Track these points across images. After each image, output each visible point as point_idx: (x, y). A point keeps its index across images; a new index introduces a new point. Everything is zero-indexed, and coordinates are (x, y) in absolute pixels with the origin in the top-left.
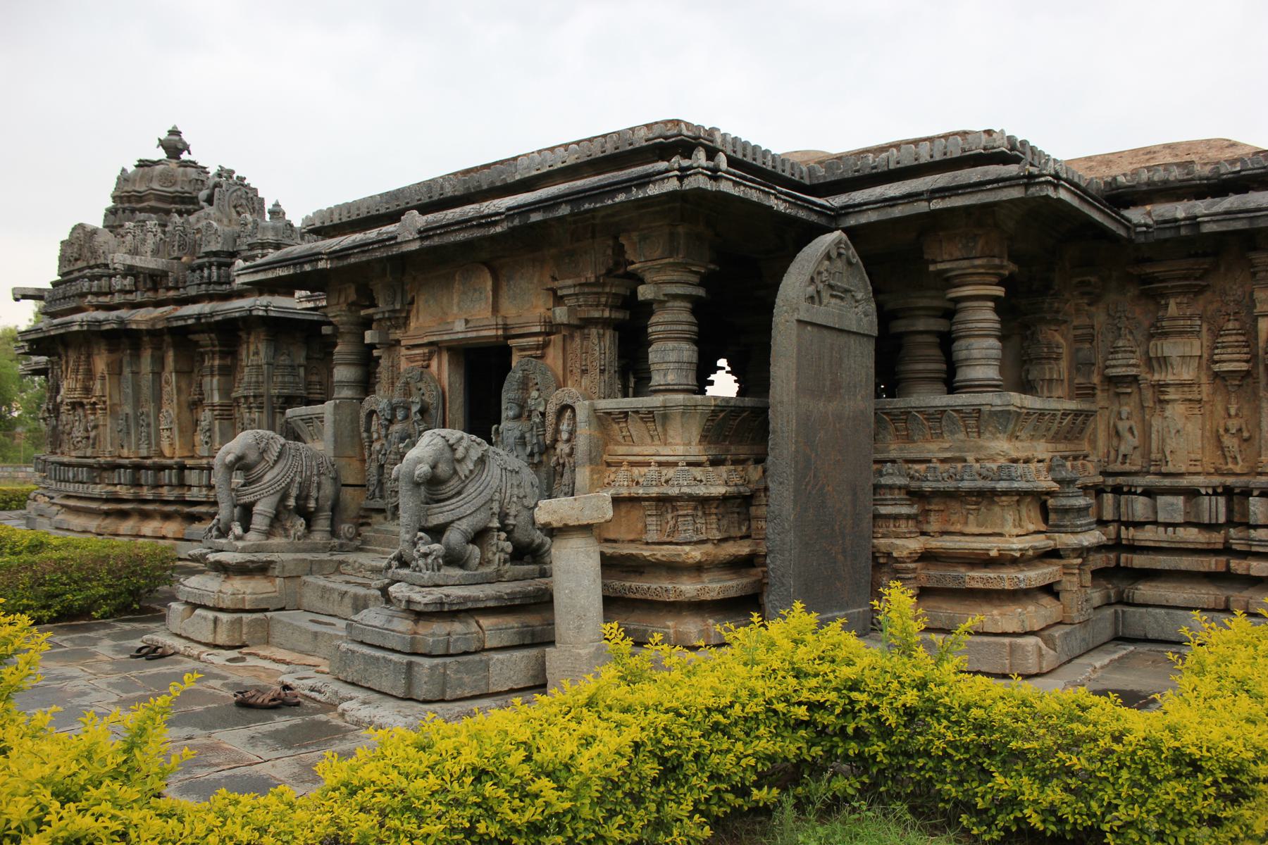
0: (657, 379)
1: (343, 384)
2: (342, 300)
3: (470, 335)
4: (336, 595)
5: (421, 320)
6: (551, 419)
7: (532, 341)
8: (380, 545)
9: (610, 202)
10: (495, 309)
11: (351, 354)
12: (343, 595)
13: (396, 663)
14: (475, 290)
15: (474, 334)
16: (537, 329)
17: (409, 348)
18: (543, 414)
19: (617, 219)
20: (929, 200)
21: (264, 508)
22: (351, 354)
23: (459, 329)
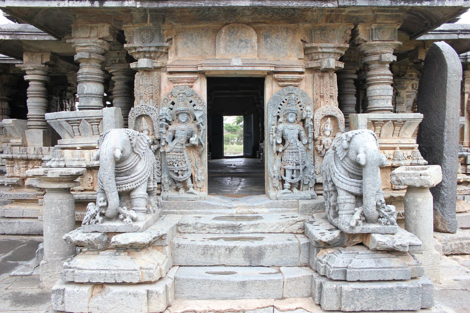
0: (374, 104)
1: (89, 96)
2: (92, 35)
3: (245, 68)
4: (223, 250)
5: (180, 55)
6: (317, 123)
7: (296, 76)
8: (175, 208)
9: (419, 5)
10: (258, 56)
11: (98, 74)
12: (230, 250)
13: (411, 289)
14: (241, 41)
15: (250, 68)
16: (300, 70)
17: (171, 73)
18: (312, 120)
19: (357, 14)
20: (458, 34)
21: (141, 192)
22: (98, 74)
23: (237, 64)
